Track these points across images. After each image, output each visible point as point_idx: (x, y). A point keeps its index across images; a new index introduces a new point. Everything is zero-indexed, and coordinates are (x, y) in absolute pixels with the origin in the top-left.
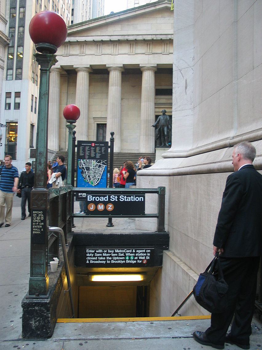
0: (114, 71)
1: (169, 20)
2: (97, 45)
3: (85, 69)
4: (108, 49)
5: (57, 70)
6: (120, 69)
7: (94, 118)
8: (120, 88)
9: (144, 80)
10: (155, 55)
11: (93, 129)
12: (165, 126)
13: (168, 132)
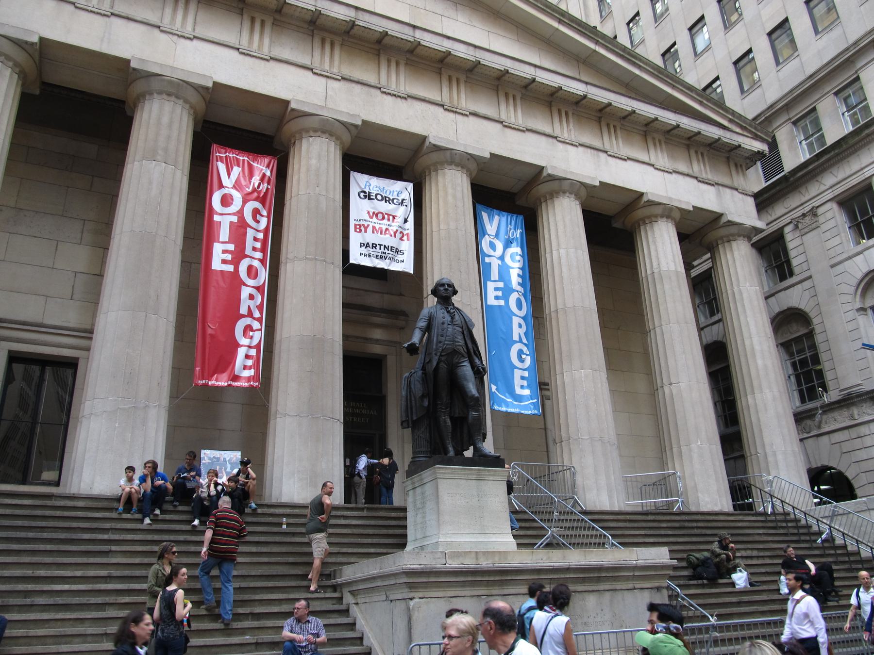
0: (165, 96)
6: (194, 98)
9: (303, 169)
10: (354, 85)
12: (463, 356)
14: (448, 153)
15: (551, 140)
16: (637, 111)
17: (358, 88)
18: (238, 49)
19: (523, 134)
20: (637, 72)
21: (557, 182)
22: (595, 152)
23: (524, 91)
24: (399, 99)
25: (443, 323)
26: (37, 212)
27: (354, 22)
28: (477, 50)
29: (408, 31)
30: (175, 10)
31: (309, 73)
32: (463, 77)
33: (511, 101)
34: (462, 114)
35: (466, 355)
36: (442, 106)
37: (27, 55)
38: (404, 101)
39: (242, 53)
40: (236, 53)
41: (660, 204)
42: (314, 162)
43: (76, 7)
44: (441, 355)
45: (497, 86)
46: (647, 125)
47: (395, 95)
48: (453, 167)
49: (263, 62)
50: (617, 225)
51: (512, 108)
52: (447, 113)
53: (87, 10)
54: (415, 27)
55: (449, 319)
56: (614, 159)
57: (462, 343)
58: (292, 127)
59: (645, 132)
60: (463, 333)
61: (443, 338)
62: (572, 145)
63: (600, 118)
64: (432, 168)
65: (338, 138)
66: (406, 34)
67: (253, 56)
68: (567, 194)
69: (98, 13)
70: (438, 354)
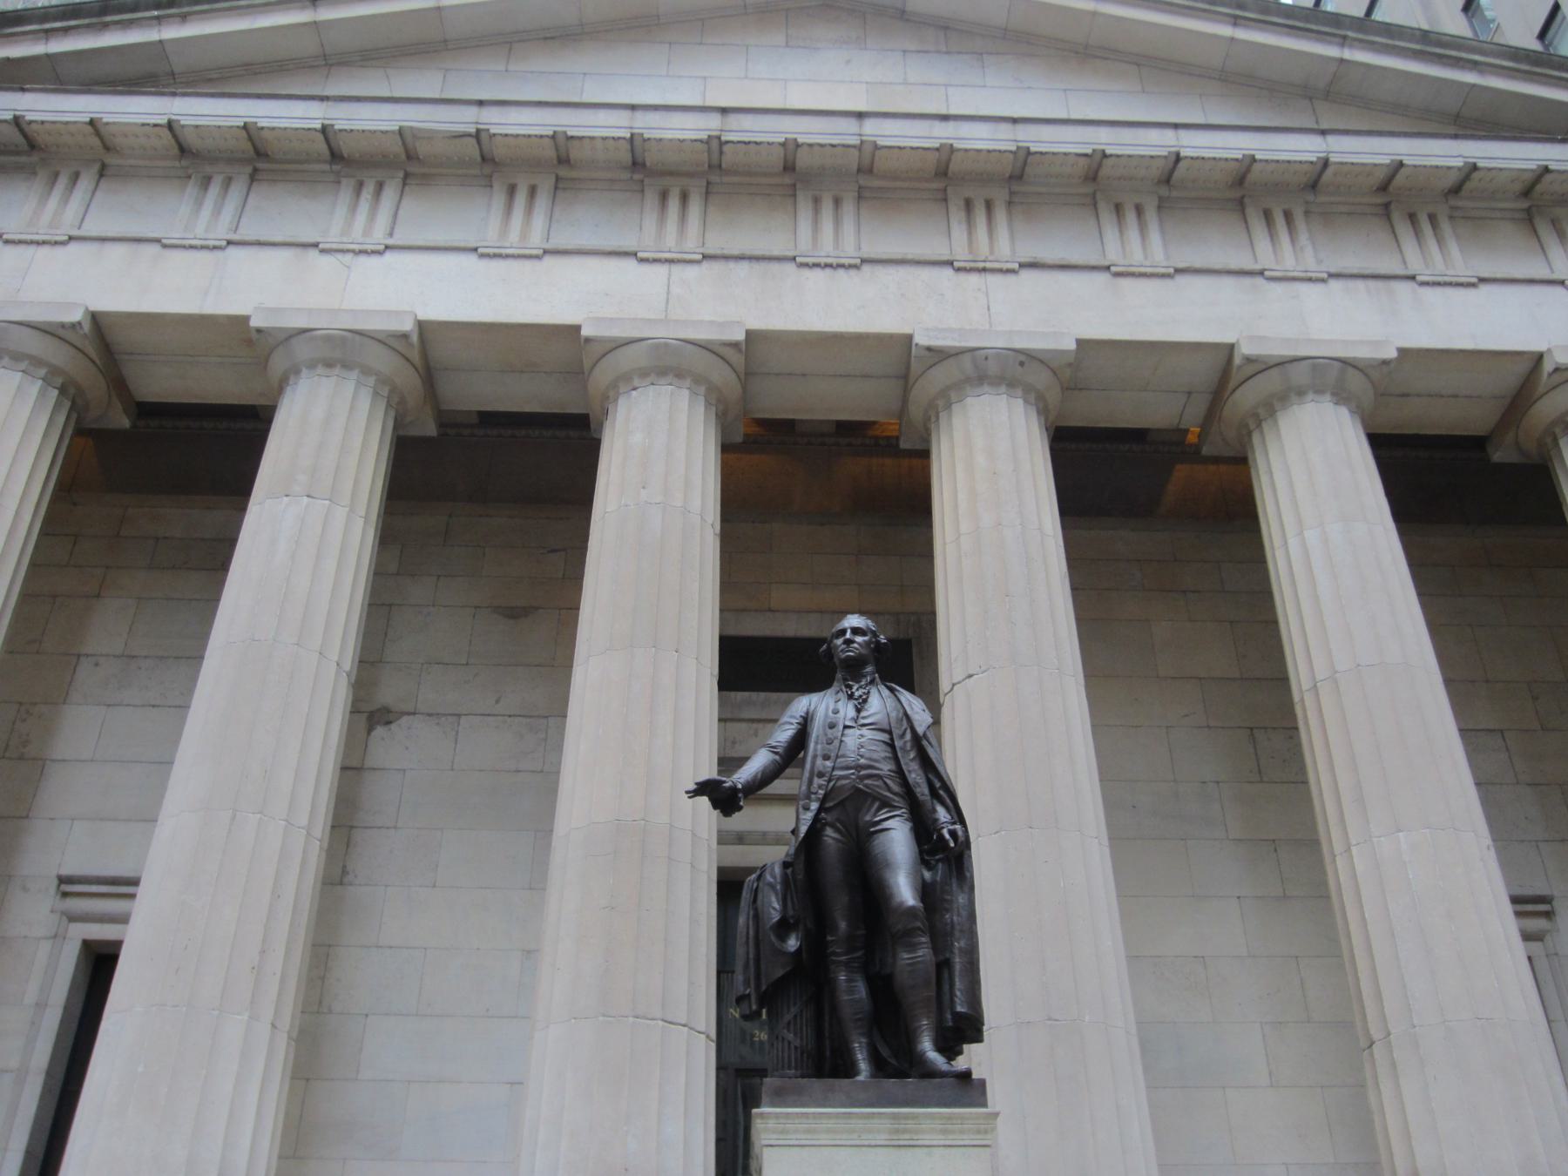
0: (320, 370)
1: (848, 62)
2: (206, 182)
7: (63, 880)
8: (359, 523)
10: (732, 265)
11: (31, 996)
12: (886, 804)
13: (926, 891)
14: (967, 358)
15: (1247, 281)
16: (1481, 164)
17: (743, 268)
18: (475, 250)
19: (1168, 282)
20: (1470, 78)
21: (1274, 372)
22: (1379, 284)
23: (1164, 191)
24: (841, 272)
25: (832, 726)
26: (161, 658)
27: (719, 138)
28: (1020, 127)
30: (353, 208)
31: (631, 264)
32: (1000, 195)
33: (1131, 217)
34: (1000, 271)
35: (898, 801)
36: (950, 263)
37: (72, 351)
38: (853, 272)
39: (482, 256)
40: (470, 260)
42: (637, 438)
43: (165, 246)
44: (820, 810)
45: (1094, 195)
46: (1527, 193)
47: (827, 266)
48: (986, 388)
49: (528, 264)
50: (1497, 456)
51: (1133, 233)
52: (963, 277)
53: (184, 247)
54: (860, 116)
55: (851, 713)
56: (1439, 291)
57: (886, 768)
58: (601, 376)
59: (1528, 210)
60: (891, 745)
61: (829, 764)
62: (1310, 280)
63: (1387, 206)
64: (941, 403)
65: (698, 380)
66: (844, 132)
67: (507, 256)
68: (1310, 396)
69: (203, 247)
70: (814, 806)
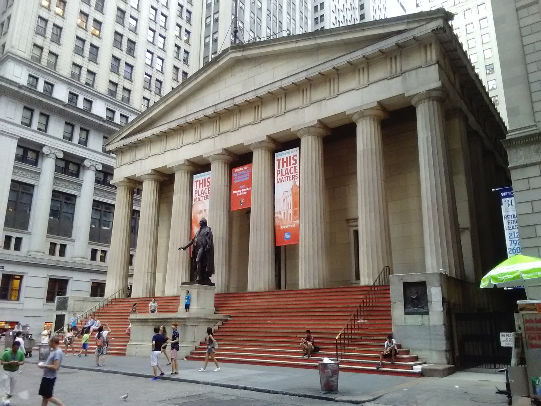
3: (147, 177)
4: (173, 143)
5: (123, 184)
6: (184, 167)
15: (296, 111)
29: (231, 101)
41: (355, 113)
54: (233, 98)
